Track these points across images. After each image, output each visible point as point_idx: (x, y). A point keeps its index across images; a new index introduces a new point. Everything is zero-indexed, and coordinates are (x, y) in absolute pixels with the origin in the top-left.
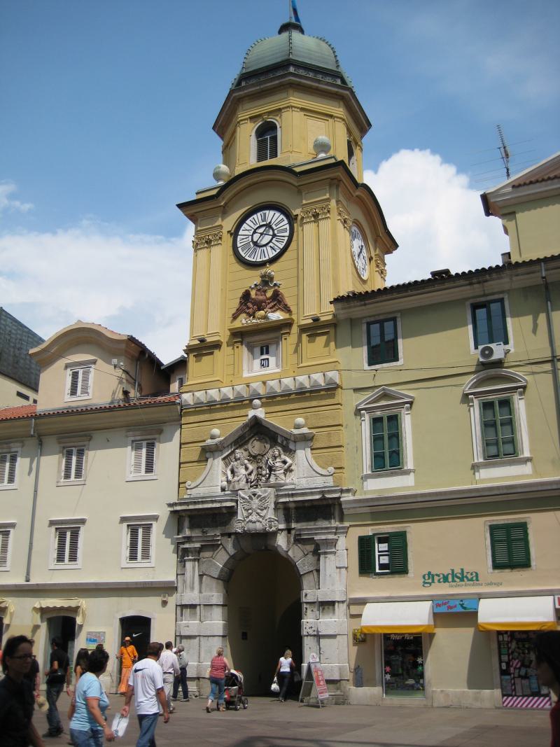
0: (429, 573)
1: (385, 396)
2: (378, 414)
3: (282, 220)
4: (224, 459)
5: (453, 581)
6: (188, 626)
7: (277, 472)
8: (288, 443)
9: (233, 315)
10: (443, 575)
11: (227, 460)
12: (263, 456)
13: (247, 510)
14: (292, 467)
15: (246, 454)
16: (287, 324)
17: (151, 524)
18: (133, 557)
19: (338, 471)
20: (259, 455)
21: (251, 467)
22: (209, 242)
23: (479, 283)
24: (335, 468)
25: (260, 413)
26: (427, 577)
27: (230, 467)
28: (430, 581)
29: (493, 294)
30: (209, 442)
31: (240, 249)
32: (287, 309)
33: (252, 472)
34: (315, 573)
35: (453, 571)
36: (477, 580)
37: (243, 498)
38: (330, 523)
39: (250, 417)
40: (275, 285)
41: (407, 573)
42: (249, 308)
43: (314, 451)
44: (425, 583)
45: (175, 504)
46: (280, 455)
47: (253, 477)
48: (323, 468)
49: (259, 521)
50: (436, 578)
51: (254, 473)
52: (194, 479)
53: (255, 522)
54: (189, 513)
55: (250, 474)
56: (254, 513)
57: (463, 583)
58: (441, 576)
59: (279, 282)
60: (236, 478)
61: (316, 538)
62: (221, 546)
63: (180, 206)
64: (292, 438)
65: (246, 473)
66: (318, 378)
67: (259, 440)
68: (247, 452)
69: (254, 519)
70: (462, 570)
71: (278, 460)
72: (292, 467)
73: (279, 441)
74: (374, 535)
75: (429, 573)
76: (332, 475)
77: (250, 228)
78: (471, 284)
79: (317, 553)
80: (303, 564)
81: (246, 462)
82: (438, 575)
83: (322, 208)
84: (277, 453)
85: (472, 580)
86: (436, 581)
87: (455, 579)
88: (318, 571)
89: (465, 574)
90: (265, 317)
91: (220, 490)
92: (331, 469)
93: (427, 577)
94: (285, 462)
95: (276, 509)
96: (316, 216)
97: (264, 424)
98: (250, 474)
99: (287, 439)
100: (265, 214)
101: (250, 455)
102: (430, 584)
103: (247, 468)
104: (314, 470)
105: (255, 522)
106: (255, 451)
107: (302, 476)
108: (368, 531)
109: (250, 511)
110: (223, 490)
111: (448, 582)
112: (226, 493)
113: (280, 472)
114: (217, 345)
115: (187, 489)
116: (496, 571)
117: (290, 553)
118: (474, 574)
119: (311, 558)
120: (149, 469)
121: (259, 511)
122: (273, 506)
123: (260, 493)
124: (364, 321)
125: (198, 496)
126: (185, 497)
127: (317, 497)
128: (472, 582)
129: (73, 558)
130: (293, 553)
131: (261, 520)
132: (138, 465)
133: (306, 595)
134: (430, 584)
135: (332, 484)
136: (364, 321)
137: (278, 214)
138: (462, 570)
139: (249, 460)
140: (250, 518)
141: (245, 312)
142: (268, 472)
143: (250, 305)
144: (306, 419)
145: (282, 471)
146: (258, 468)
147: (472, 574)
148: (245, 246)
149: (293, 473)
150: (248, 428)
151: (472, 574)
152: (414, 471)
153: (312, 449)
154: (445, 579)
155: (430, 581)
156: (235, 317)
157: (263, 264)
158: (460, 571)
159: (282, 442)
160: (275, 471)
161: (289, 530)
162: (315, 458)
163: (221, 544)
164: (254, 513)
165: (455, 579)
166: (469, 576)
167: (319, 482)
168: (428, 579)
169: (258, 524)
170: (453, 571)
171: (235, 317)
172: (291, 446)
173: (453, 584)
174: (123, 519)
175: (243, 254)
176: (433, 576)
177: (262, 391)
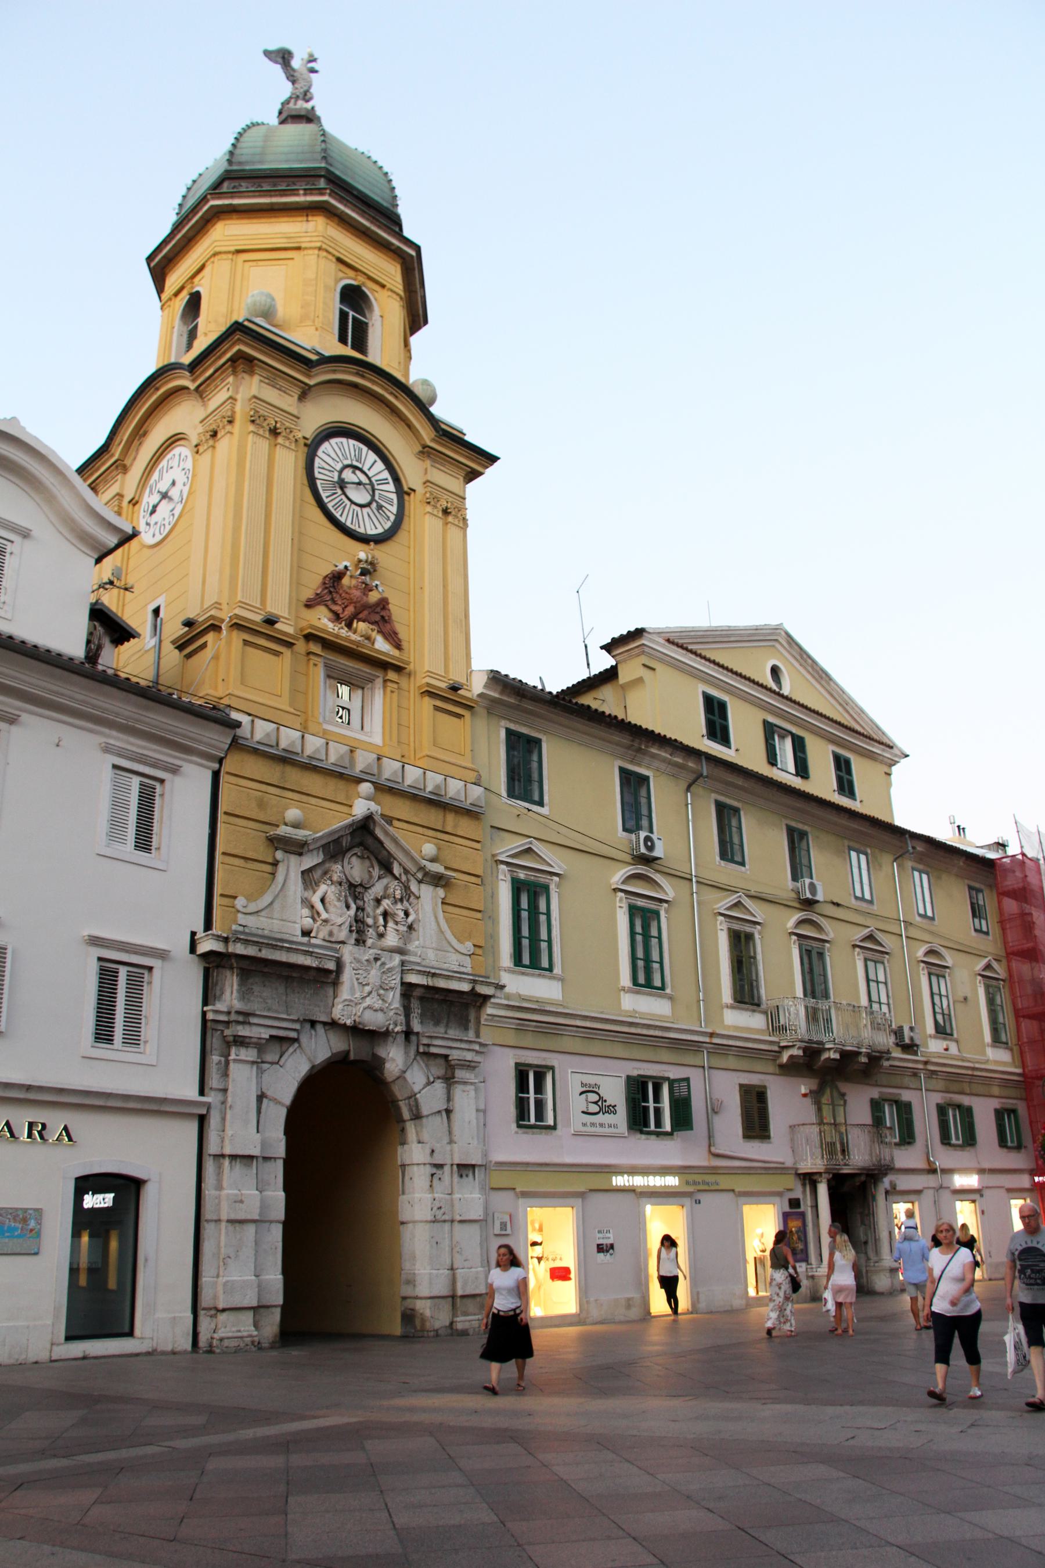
1: (529, 851)
3: (384, 482)
4: (303, 872)
6: (241, 1202)
8: (408, 880)
9: (309, 600)
12: (366, 889)
17: (150, 969)
18: (103, 1034)
20: (361, 885)
24: (475, 946)
27: (319, 894)
32: (398, 646)
34: (444, 1114)
42: (334, 602)
43: (446, 907)
46: (401, 900)
48: (459, 941)
49: (382, 1010)
52: (250, 898)
53: (376, 1010)
54: (245, 964)
56: (374, 994)
61: (455, 1055)
62: (296, 1045)
66: (454, 789)
67: (362, 857)
71: (399, 906)
73: (397, 870)
76: (470, 955)
79: (449, 1080)
80: (431, 1098)
88: (448, 1112)
91: (299, 933)
92: (469, 945)
99: (406, 872)
105: (376, 1010)
109: (367, 989)
112: (313, 941)
119: (439, 1086)
120: (144, 841)
121: (382, 992)
125: (260, 932)
132: (116, 824)
135: (469, 970)
140: (368, 1001)
141: (327, 606)
142: (381, 921)
143: (337, 597)
159: (400, 875)
162: (447, 921)
164: (374, 994)
167: (453, 962)
169: (380, 1015)
171: (309, 605)
174: (95, 941)
175: (324, 495)
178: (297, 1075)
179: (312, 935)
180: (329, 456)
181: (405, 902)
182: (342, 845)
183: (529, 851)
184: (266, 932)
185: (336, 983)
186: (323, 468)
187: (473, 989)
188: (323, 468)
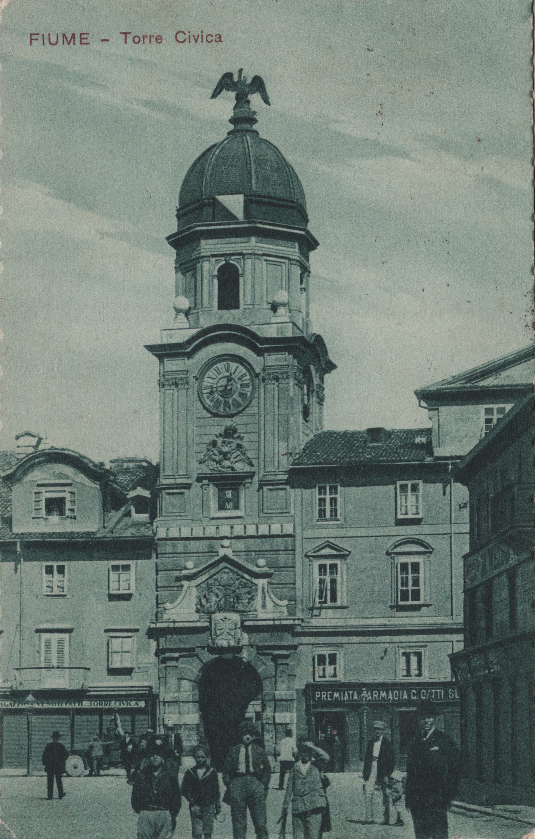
7: (243, 601)
11: (198, 587)
16: (251, 475)
25: (229, 553)
33: (221, 598)
38: (282, 639)
55: (220, 600)
59: (242, 435)
63: (151, 348)
65: (218, 600)
77: (214, 377)
83: (282, 373)
98: (220, 600)
100: (229, 365)
103: (217, 596)
137: (241, 368)
145: (247, 601)
160: (241, 600)
180: (211, 378)
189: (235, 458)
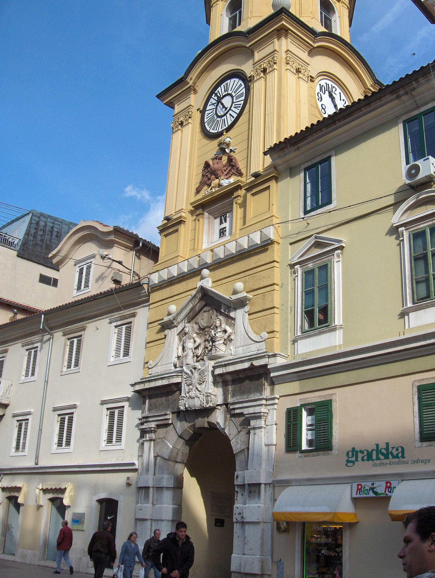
0: (353, 449)
2: (310, 265)
5: (378, 458)
6: (141, 510)
10: (368, 451)
13: (188, 385)
14: (232, 337)
15: (196, 327)
19: (271, 335)
20: (207, 327)
21: (198, 341)
22: (181, 124)
23: (406, 93)
24: (268, 333)
26: (350, 455)
28: (353, 459)
29: (426, 103)
30: (166, 319)
31: (206, 124)
33: (199, 345)
35: (377, 445)
36: (403, 457)
37: (186, 373)
39: (198, 287)
40: (231, 151)
41: (331, 450)
44: (348, 461)
45: (136, 384)
47: (199, 351)
50: (360, 455)
51: (202, 347)
55: (197, 348)
57: (387, 461)
58: (365, 453)
60: (185, 353)
61: (246, 411)
62: (172, 426)
64: (232, 306)
68: (198, 326)
69: (193, 395)
70: (387, 444)
72: (232, 337)
74: (302, 406)
75: (353, 449)
76: (265, 340)
78: (398, 97)
81: (195, 335)
82: (362, 452)
84: (218, 322)
85: (397, 457)
86: (360, 459)
87: (380, 456)
89: (390, 449)
90: (220, 185)
91: (173, 368)
92: (265, 335)
93: (350, 455)
94: (225, 331)
95: (215, 383)
96: (264, 71)
97: (210, 294)
98: (197, 348)
101: (200, 329)
102: (353, 462)
104: (249, 337)
105: (194, 398)
106: (203, 323)
107: (238, 345)
108: (295, 402)
109: (191, 387)
110: (175, 366)
111: (373, 460)
113: (219, 343)
114: (180, 222)
115: (149, 369)
116: (425, 444)
117: (226, 431)
118: (400, 449)
122: (211, 379)
123: (200, 367)
124: (303, 167)
125: (156, 374)
126: (147, 376)
127: (246, 365)
128: (396, 460)
129: (68, 443)
130: (229, 430)
131: (199, 395)
132: (118, 349)
133: (237, 477)
134: (353, 462)
136: (303, 167)
137: (237, 80)
138: (387, 444)
139: (197, 333)
144: (245, 283)
145: (222, 342)
146: (205, 341)
147: (397, 450)
148: (212, 120)
149: (233, 341)
150: (197, 300)
151: (397, 450)
152: (341, 327)
153: (249, 315)
154: (369, 457)
155: (353, 459)
156: (198, 191)
157: (220, 134)
158: (385, 446)
161: (226, 404)
162: (251, 324)
163: (172, 424)
165: (380, 456)
166: (395, 452)
168: (352, 457)
170: (377, 445)
172: (232, 314)
173: (378, 462)
174: (103, 403)
175: (208, 128)
176: (357, 452)
177: (209, 260)
178: (172, 442)
179: (177, 366)
181: (223, 326)
182: (196, 310)
183: (317, 245)
184: (159, 374)
185: (180, 390)
186: (209, 113)
187: (252, 364)
188: (209, 113)
189: (226, 175)
